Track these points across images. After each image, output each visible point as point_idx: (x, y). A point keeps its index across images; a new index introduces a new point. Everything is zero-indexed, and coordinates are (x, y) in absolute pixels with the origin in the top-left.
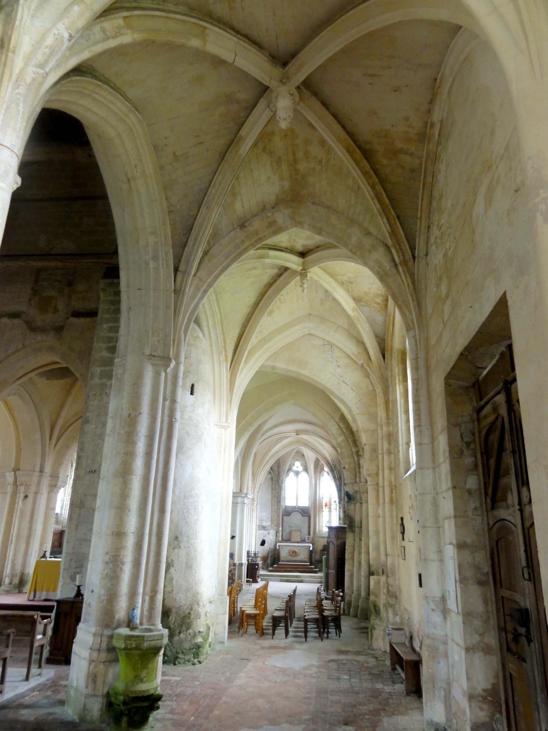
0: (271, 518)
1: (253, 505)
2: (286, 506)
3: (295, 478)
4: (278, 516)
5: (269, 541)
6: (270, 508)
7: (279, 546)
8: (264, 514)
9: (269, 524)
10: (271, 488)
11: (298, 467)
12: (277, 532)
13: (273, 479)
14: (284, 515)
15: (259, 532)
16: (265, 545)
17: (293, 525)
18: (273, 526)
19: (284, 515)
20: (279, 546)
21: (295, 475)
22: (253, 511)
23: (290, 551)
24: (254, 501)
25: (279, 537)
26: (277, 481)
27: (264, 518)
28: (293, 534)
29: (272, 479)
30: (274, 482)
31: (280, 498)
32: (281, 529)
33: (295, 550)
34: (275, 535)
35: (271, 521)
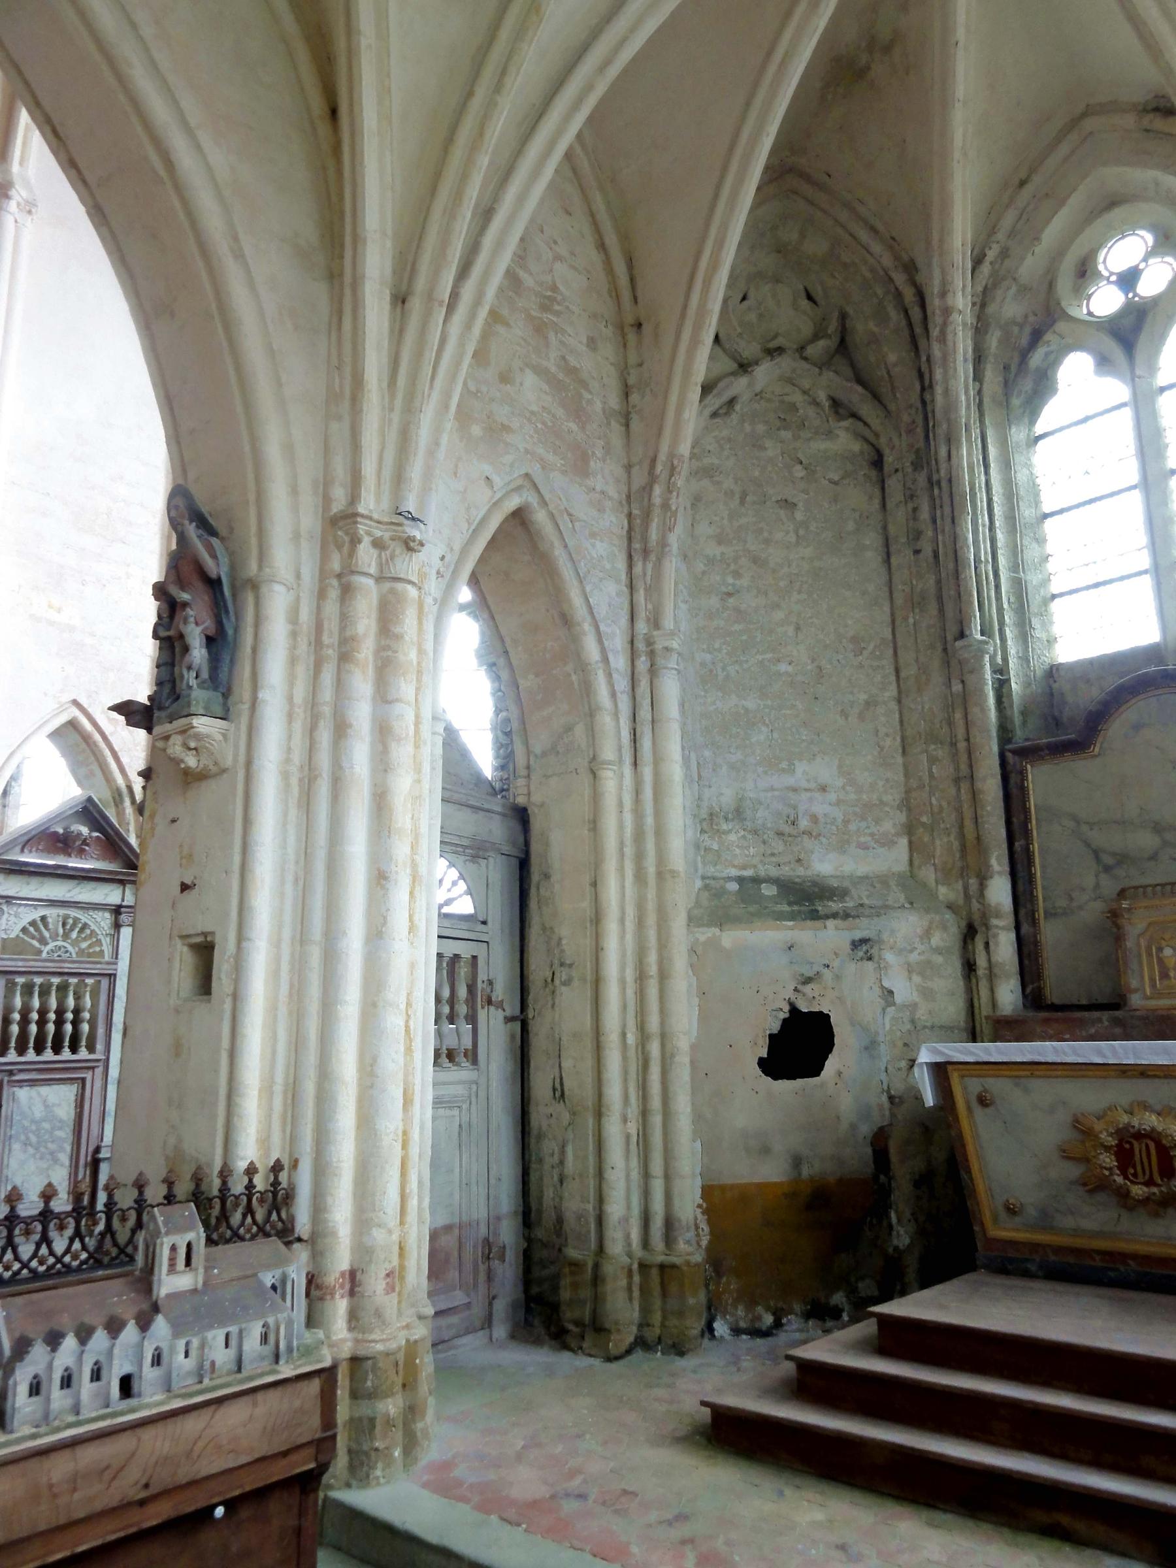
0: (906, 804)
1: (347, 591)
2: (1053, 672)
3: (1116, 389)
4: (967, 778)
5: (886, 1024)
6: (886, 717)
7: (940, 1070)
8: (824, 770)
9: (896, 858)
10: (872, 539)
11: (1128, 279)
12: (970, 933)
13: (889, 459)
14: (1030, 753)
15: (730, 938)
16: (831, 1065)
17: (1146, 841)
18: (928, 874)
19: (1030, 753)
20: (940, 1070)
21: (1104, 363)
22: (345, 657)
23: (1082, 1128)
24: (355, 541)
25: (991, 976)
26: (923, 459)
27: (821, 807)
28: (1136, 927)
29: (878, 462)
30: (894, 484)
31: (960, 596)
32: (1000, 892)
33: (1151, 1121)
34: (954, 967)
35: (909, 829)
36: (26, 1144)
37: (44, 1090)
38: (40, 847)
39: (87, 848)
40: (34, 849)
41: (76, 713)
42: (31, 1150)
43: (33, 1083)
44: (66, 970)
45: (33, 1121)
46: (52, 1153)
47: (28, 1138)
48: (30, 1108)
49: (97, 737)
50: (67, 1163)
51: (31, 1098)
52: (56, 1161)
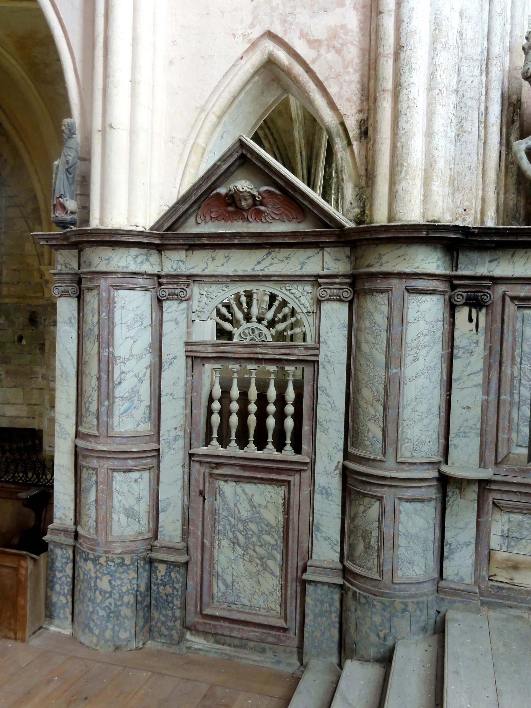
36: (234, 543)
37: (250, 488)
38: (213, 215)
39: (262, 208)
40: (208, 218)
41: (270, 46)
42: (240, 551)
43: (238, 479)
44: (260, 356)
45: (239, 520)
46: (261, 558)
47: (235, 537)
48: (236, 505)
49: (298, 70)
50: (278, 572)
51: (236, 494)
52: (265, 567)
